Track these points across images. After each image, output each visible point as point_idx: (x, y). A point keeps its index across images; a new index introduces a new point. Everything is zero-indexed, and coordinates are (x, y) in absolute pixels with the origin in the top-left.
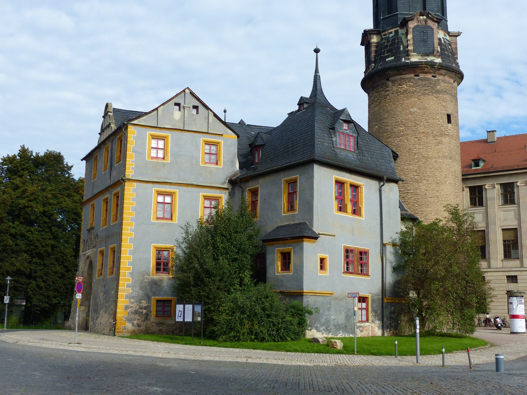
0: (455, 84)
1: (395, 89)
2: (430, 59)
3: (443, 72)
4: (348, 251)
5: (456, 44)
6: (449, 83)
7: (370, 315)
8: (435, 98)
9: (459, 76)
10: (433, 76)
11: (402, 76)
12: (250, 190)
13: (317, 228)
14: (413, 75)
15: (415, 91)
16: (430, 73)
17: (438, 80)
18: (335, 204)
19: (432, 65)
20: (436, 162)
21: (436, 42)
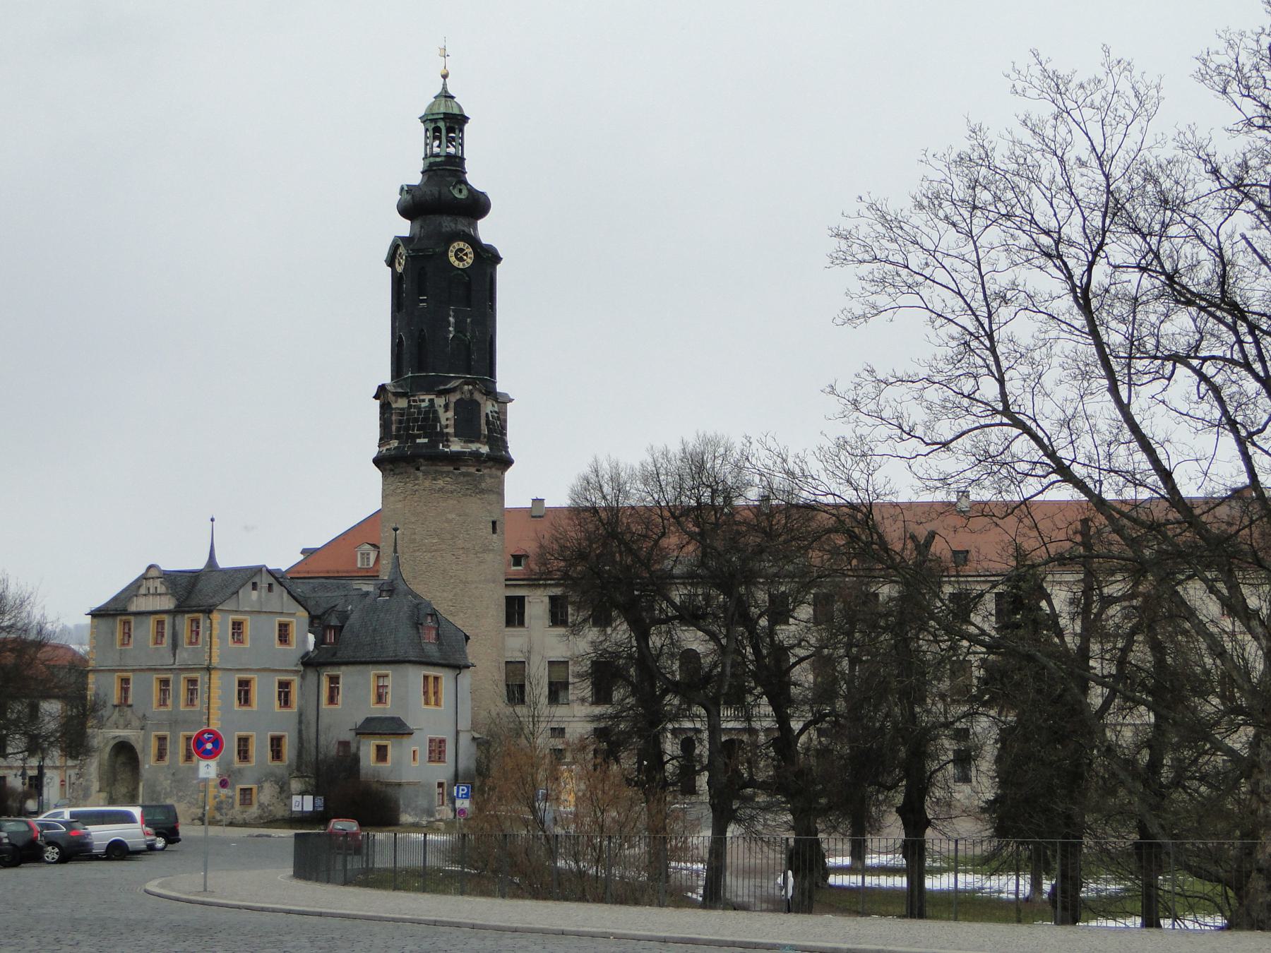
0: (499, 473)
1: (427, 483)
2: (474, 447)
3: (489, 464)
4: (431, 741)
5: (505, 413)
6: (497, 477)
7: (445, 798)
8: (479, 501)
9: (508, 462)
10: (478, 470)
11: (438, 468)
12: (328, 675)
13: (411, 724)
14: (451, 468)
15: (455, 490)
16: (474, 466)
17: (483, 475)
18: (423, 698)
19: (476, 455)
20: (476, 588)
21: (483, 421)
